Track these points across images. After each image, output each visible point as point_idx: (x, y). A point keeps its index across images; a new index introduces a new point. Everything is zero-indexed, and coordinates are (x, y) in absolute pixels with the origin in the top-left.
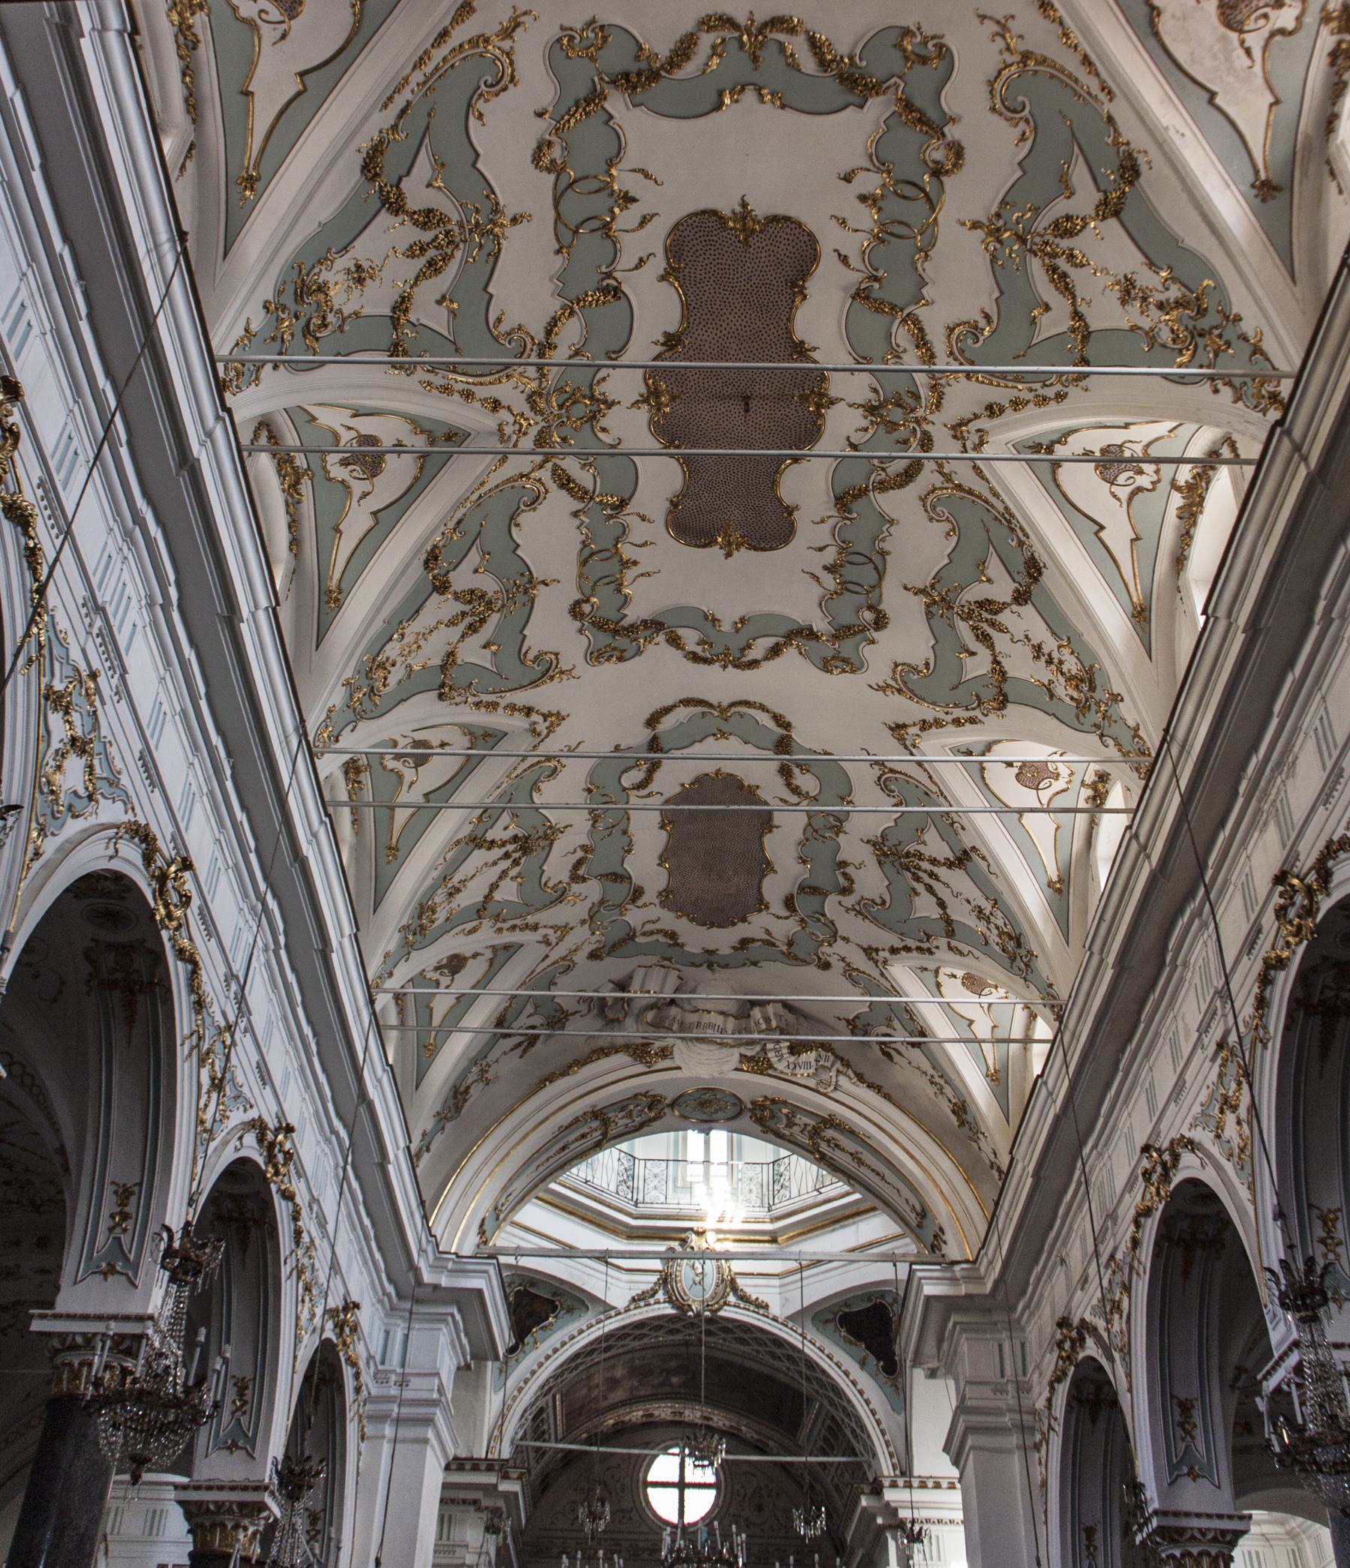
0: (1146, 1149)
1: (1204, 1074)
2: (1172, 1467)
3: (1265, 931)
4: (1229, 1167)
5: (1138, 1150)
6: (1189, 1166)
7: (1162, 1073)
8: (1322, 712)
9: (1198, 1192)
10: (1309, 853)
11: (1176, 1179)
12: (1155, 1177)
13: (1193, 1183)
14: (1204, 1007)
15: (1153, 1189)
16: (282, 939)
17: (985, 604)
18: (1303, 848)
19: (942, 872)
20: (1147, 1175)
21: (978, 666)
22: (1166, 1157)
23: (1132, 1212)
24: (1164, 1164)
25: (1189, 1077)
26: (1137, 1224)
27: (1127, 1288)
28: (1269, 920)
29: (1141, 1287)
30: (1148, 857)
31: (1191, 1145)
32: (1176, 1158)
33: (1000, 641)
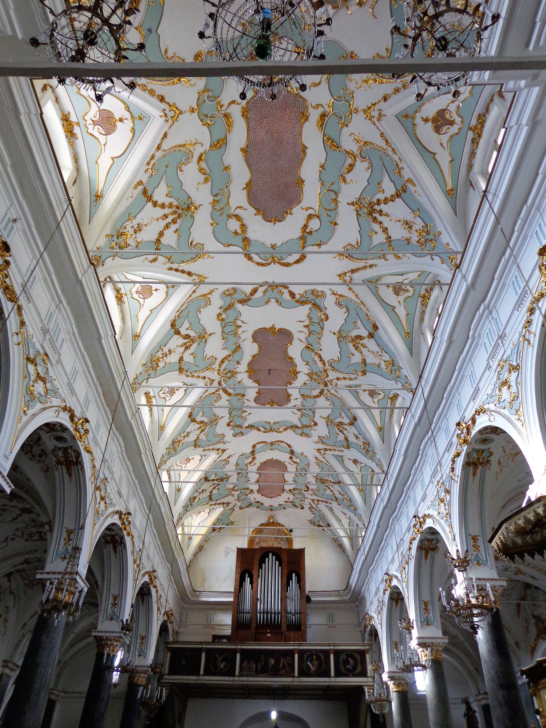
0: (415, 517)
1: (432, 492)
2: (422, 622)
3: (454, 443)
4: (442, 521)
5: (412, 517)
6: (429, 523)
7: (419, 493)
8: (472, 369)
9: (432, 531)
10: (469, 415)
11: (425, 527)
12: (417, 526)
13: (430, 528)
14: (433, 469)
15: (416, 530)
16: (124, 449)
17: (359, 337)
18: (466, 414)
19: (346, 427)
20: (415, 526)
21: (357, 358)
22: (421, 520)
23: (409, 539)
24: (421, 523)
25: (428, 492)
26: (411, 543)
27: (407, 563)
28: (455, 439)
29: (412, 563)
30: (414, 419)
31: (429, 516)
32: (425, 521)
33: (364, 350)
